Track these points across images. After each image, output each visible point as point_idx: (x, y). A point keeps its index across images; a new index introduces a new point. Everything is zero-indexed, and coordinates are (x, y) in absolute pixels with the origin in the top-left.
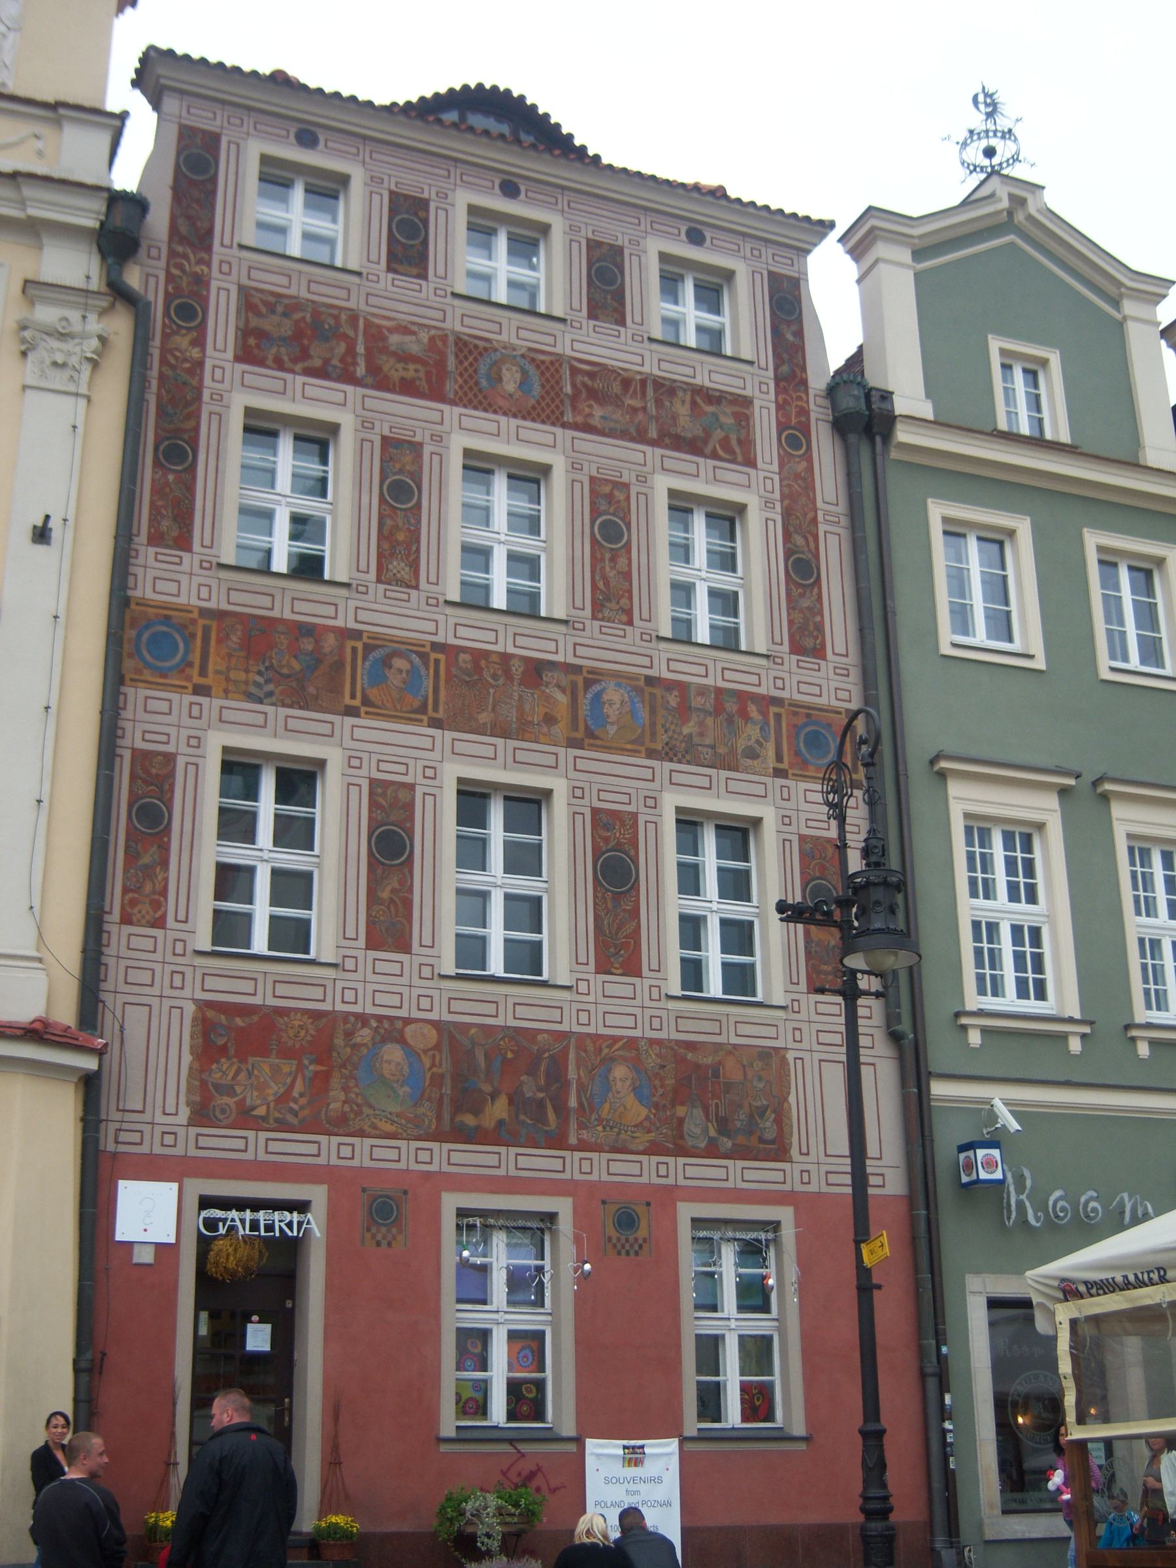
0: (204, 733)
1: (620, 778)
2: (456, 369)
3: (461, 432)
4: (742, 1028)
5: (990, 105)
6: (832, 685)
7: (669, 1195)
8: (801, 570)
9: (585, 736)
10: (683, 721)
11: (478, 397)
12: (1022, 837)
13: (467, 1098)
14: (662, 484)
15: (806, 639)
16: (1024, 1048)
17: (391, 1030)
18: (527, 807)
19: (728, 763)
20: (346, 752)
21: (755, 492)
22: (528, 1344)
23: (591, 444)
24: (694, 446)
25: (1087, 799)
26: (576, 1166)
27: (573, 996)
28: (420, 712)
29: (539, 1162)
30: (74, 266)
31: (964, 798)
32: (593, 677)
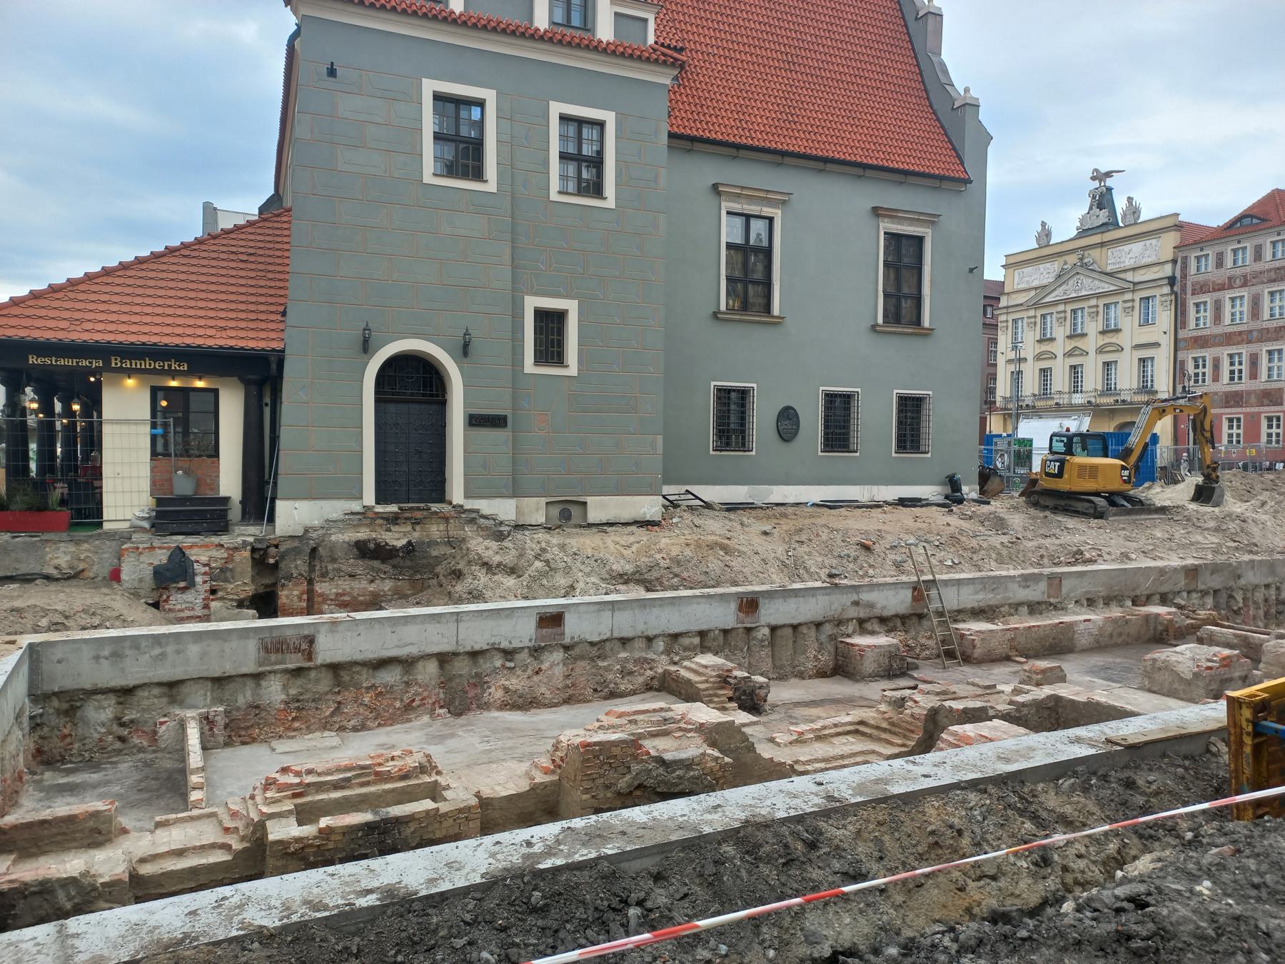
0: (1188, 357)
1: (1254, 348)
2: (1229, 284)
3: (1228, 294)
7: (1259, 414)
9: (1249, 342)
13: (1227, 402)
14: (1266, 291)
17: (1216, 393)
19: (1277, 340)
20: (1208, 354)
22: (1238, 435)
23: (1253, 288)
24: (1274, 281)
26: (1244, 410)
28: (1221, 345)
29: (1239, 410)
30: (1167, 290)
32: (1251, 331)
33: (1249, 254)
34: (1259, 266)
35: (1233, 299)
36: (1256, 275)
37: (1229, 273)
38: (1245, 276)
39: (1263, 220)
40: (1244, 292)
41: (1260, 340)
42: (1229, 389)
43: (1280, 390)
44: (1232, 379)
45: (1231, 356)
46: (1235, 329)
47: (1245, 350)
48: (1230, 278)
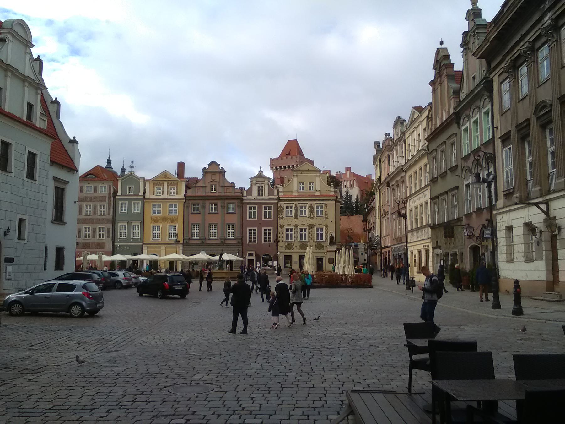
1: (94, 226)
3: (85, 204)
4: (103, 241)
5: (132, 162)
6: (111, 217)
8: (109, 209)
10: (99, 221)
11: (86, 201)
12: (125, 226)
15: (109, 214)
16: (122, 241)
18: (89, 228)
21: (106, 204)
24: (102, 201)
25: (129, 223)
27: (91, 240)
28: (82, 223)
31: (120, 224)
32: (93, 219)
33: (93, 189)
34: (96, 195)
35: (86, 206)
36: (95, 198)
37: (85, 195)
38: (91, 197)
39: (97, 177)
40: (91, 203)
41: (97, 223)
42: (84, 241)
43: (103, 243)
44: (100, 237)
45: (85, 228)
46: (100, 217)
47: (91, 226)
48: (86, 197)
